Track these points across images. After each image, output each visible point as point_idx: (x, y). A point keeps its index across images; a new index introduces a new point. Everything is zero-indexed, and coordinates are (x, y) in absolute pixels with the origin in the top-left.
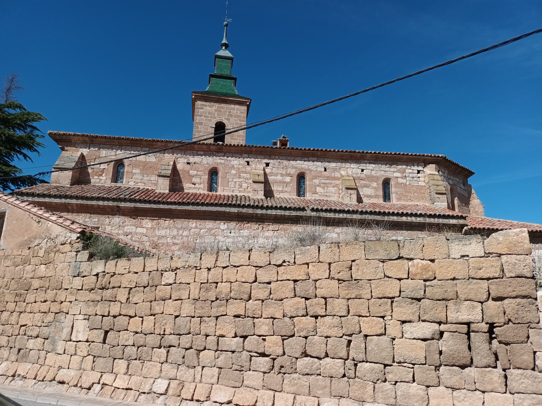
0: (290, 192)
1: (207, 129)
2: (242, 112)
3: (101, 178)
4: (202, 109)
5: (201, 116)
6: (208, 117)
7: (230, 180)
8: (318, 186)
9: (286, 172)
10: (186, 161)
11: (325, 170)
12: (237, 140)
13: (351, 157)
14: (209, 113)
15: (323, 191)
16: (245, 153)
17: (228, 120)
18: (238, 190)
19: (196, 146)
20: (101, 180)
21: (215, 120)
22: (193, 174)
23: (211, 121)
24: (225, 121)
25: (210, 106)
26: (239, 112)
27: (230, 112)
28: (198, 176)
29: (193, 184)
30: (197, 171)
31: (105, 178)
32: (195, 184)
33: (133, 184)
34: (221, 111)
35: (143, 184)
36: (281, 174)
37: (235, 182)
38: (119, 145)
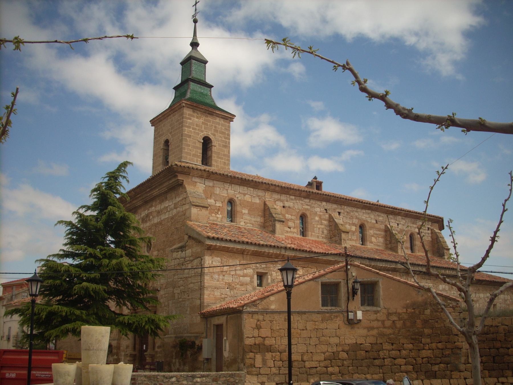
0: (356, 241)
1: (195, 143)
2: (226, 129)
3: (218, 216)
4: (190, 119)
5: (189, 127)
6: (196, 129)
7: (315, 226)
8: (373, 236)
9: (352, 222)
10: (282, 205)
11: (377, 222)
12: (223, 159)
13: (392, 212)
14: (197, 125)
15: (376, 241)
16: (325, 201)
17: (214, 135)
18: (321, 236)
19: (291, 192)
20: (218, 218)
21: (202, 134)
22: (289, 218)
23: (198, 134)
24: (211, 137)
25: (197, 118)
26: (223, 128)
27: (215, 127)
28: (292, 221)
29: (289, 228)
30: (291, 215)
31: (221, 216)
32: (290, 228)
33: (244, 224)
34: (207, 125)
35: (252, 225)
36: (349, 223)
37: (319, 228)
38: (230, 183)
